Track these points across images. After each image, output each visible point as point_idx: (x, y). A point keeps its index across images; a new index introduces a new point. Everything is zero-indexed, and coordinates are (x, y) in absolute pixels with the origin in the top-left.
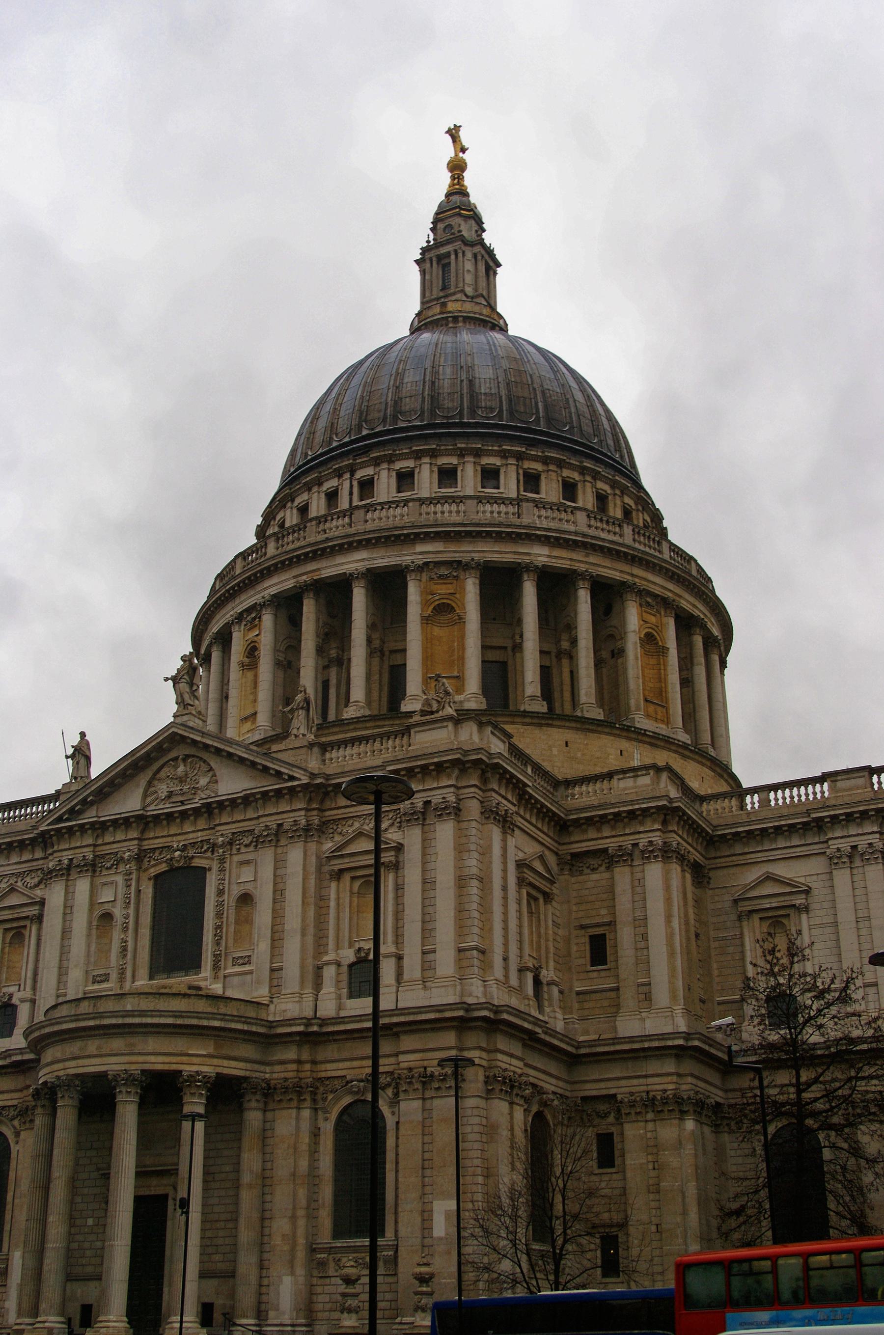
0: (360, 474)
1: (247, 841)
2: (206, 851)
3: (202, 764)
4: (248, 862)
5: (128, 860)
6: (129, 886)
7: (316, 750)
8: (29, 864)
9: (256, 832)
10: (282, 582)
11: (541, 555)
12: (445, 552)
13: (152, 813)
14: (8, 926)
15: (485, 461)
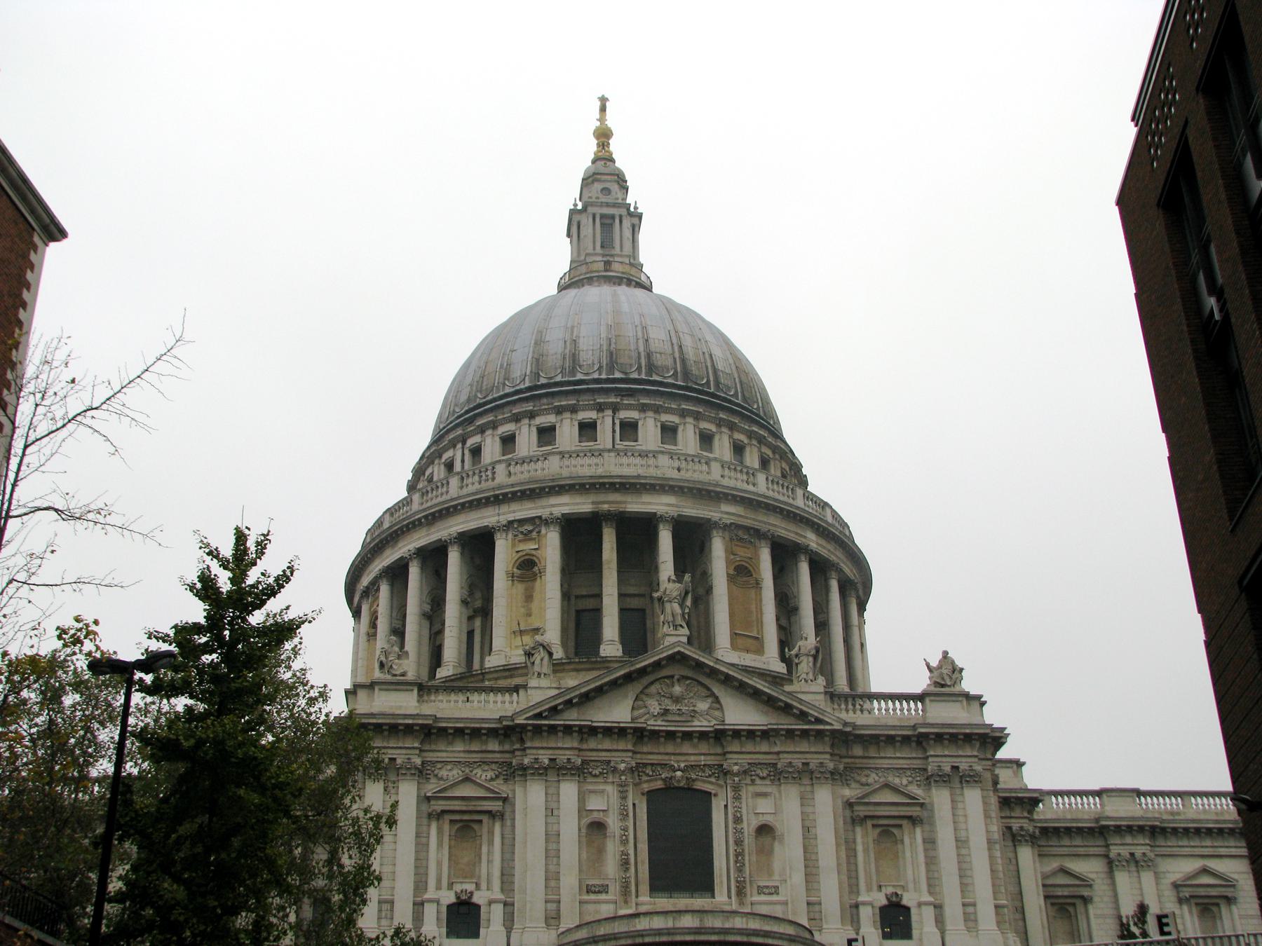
0: (623, 414)
1: (765, 773)
2: (710, 776)
3: (699, 688)
4: (764, 795)
5: (624, 771)
6: (624, 798)
7: (828, 697)
8: (479, 755)
9: (779, 766)
10: (577, 504)
11: (811, 540)
12: (747, 518)
13: (653, 728)
14: (457, 817)
15: (738, 436)
